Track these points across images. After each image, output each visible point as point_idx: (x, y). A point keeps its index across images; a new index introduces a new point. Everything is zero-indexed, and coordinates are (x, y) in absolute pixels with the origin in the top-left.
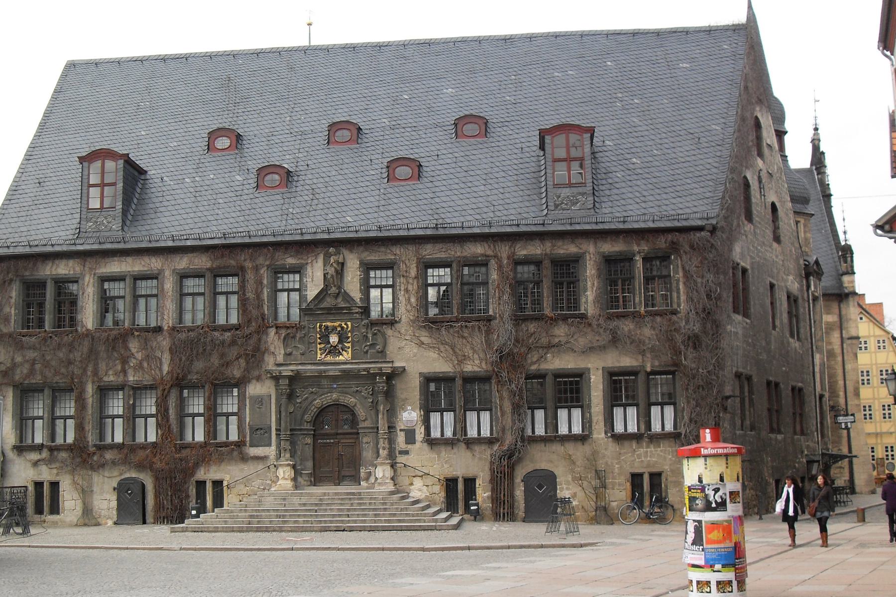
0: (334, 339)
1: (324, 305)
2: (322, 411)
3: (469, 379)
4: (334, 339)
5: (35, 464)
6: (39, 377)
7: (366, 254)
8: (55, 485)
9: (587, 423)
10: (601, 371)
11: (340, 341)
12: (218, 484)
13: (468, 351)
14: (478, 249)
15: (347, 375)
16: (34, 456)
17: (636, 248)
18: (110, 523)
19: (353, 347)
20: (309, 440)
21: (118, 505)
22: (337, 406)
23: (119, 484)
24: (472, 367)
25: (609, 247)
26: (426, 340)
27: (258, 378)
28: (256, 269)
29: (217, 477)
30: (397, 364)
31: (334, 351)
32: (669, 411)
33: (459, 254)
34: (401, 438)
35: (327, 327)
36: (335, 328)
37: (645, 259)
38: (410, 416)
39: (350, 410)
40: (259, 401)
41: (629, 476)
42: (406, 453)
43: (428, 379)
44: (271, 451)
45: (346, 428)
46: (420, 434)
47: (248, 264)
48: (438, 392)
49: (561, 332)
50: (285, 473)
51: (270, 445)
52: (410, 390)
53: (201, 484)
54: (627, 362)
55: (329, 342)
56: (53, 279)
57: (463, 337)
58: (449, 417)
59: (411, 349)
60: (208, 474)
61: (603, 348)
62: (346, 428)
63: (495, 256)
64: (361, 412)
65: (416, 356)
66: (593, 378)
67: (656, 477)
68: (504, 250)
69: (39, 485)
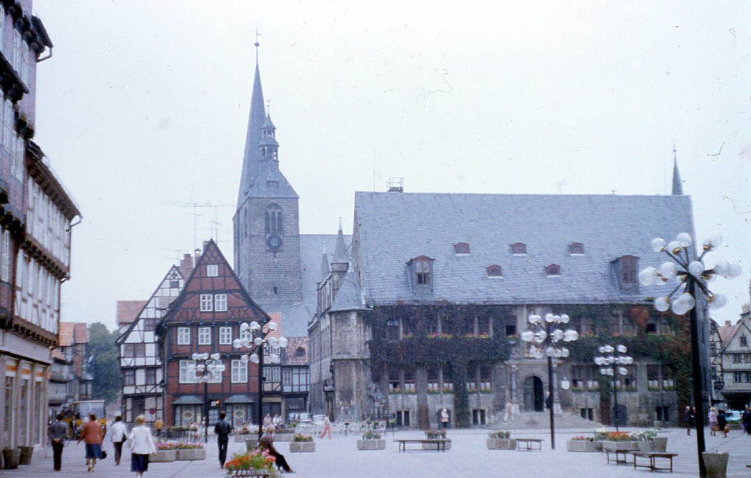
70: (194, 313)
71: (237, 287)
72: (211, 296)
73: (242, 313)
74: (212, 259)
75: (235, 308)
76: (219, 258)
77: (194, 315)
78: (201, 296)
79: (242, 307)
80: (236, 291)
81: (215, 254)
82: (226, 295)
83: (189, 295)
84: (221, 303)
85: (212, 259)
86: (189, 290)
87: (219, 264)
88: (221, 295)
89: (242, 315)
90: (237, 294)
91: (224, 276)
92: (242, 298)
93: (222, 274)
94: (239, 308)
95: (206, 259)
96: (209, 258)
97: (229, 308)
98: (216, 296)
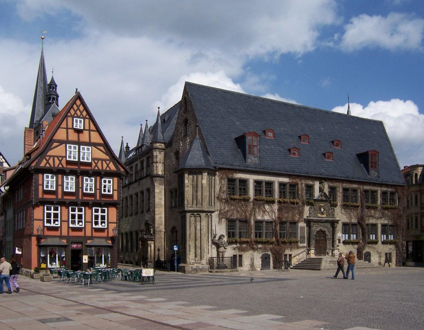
0: (322, 210)
1: (319, 199)
2: (318, 232)
3: (354, 225)
4: (322, 210)
5: (234, 249)
6: (236, 216)
7: (330, 183)
8: (241, 256)
9: (376, 238)
10: (380, 224)
11: (324, 211)
12: (290, 255)
13: (353, 217)
14: (355, 186)
15: (326, 221)
16: (234, 246)
17: (388, 189)
18: (259, 269)
19: (326, 213)
20: (314, 242)
21: (262, 263)
22: (321, 231)
23: (262, 256)
24: (354, 221)
25: (385, 189)
26: (343, 212)
27: (302, 221)
28: (302, 184)
29: (290, 253)
30: (337, 219)
31: (322, 213)
32: (392, 236)
33: (351, 186)
34: (337, 241)
35: (320, 206)
36: (323, 206)
37: (390, 194)
38: (339, 235)
39: (324, 232)
40: (302, 228)
41: (385, 254)
42: (338, 246)
43: (345, 225)
44: (305, 245)
45: (322, 238)
46: (341, 241)
47: (300, 183)
48: (347, 228)
49: (373, 212)
50: (312, 251)
51: (305, 243)
52: (339, 227)
53: (286, 255)
54: (386, 222)
55: (321, 210)
56: (239, 179)
57: (352, 212)
58: (347, 235)
59: (340, 214)
60: (287, 252)
61: (381, 218)
62: (322, 238)
63: (360, 188)
64: (327, 233)
65: (341, 216)
66: (379, 226)
67: (390, 254)
68: (361, 187)
69: (235, 256)
70: (60, 161)
71: (101, 141)
72: (77, 146)
73: (105, 165)
74: (78, 113)
75: (98, 160)
76: (84, 113)
77: (60, 163)
78: (68, 145)
79: (105, 160)
80: (100, 145)
81: (81, 108)
82: (90, 148)
83: (55, 144)
84: (87, 154)
85: (78, 113)
86: (55, 138)
87: (84, 118)
88: (86, 147)
89: (104, 169)
90: (102, 148)
91: (90, 130)
92: (104, 150)
93: (87, 127)
94: (102, 160)
95: (72, 112)
96: (76, 113)
97: (92, 159)
98: (81, 147)
